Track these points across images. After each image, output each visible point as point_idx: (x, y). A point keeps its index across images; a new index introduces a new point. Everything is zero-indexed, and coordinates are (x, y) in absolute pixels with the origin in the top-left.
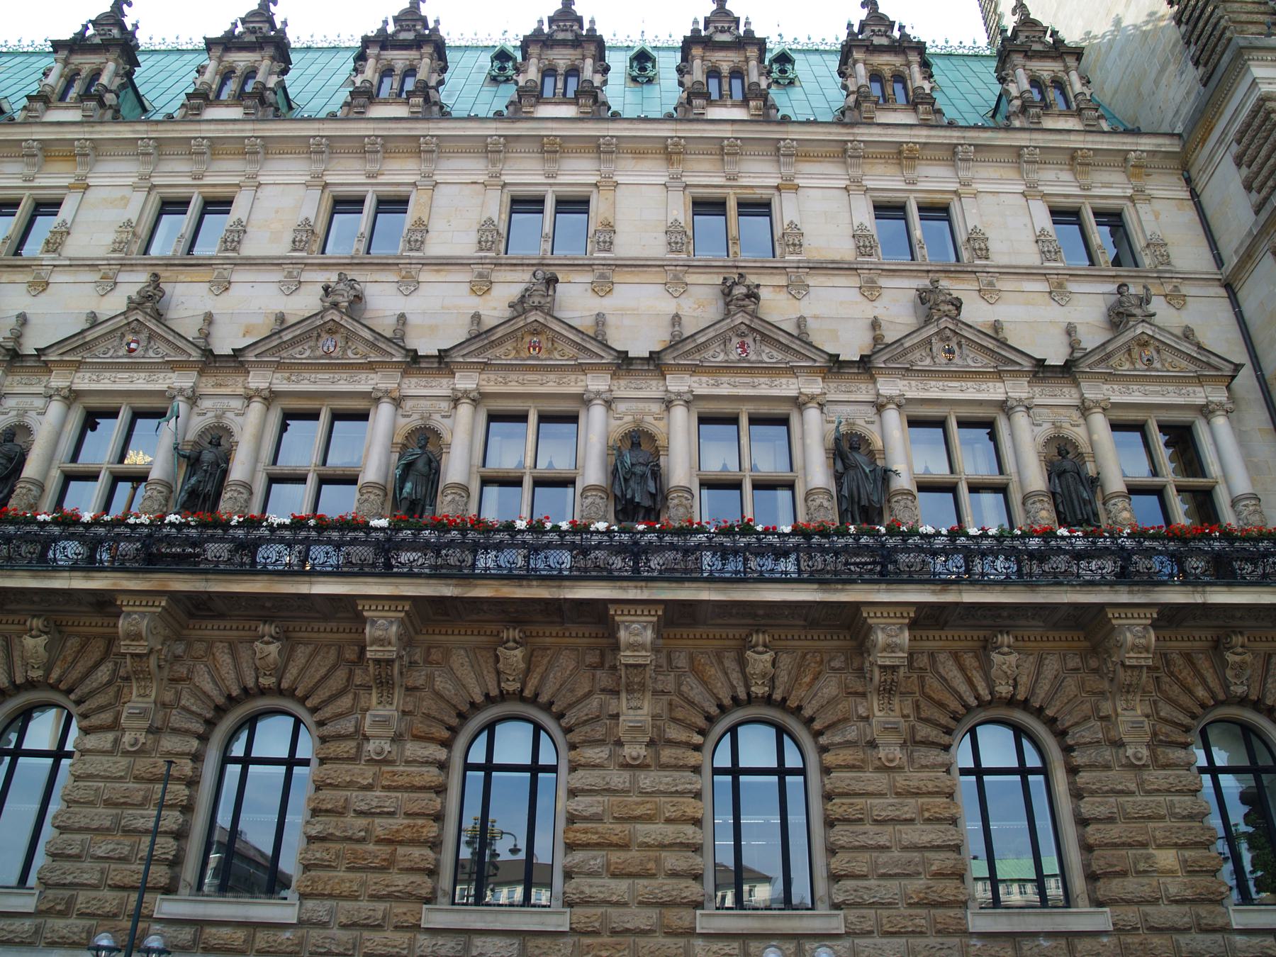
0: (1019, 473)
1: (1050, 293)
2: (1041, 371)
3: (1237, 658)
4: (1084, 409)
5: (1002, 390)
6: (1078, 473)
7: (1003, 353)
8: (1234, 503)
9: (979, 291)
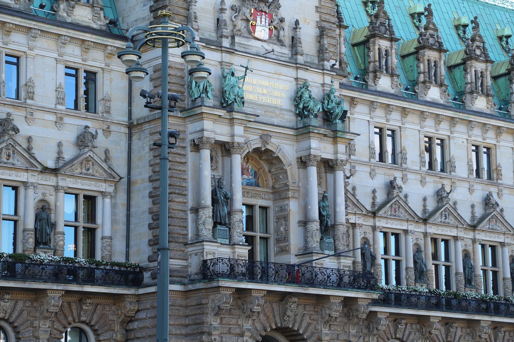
0: (24, 220)
1: (56, 122)
2: (45, 170)
3: (87, 308)
4: (57, 188)
5: (26, 177)
6: (48, 219)
7: (31, 160)
8: (103, 238)
9: (26, 117)
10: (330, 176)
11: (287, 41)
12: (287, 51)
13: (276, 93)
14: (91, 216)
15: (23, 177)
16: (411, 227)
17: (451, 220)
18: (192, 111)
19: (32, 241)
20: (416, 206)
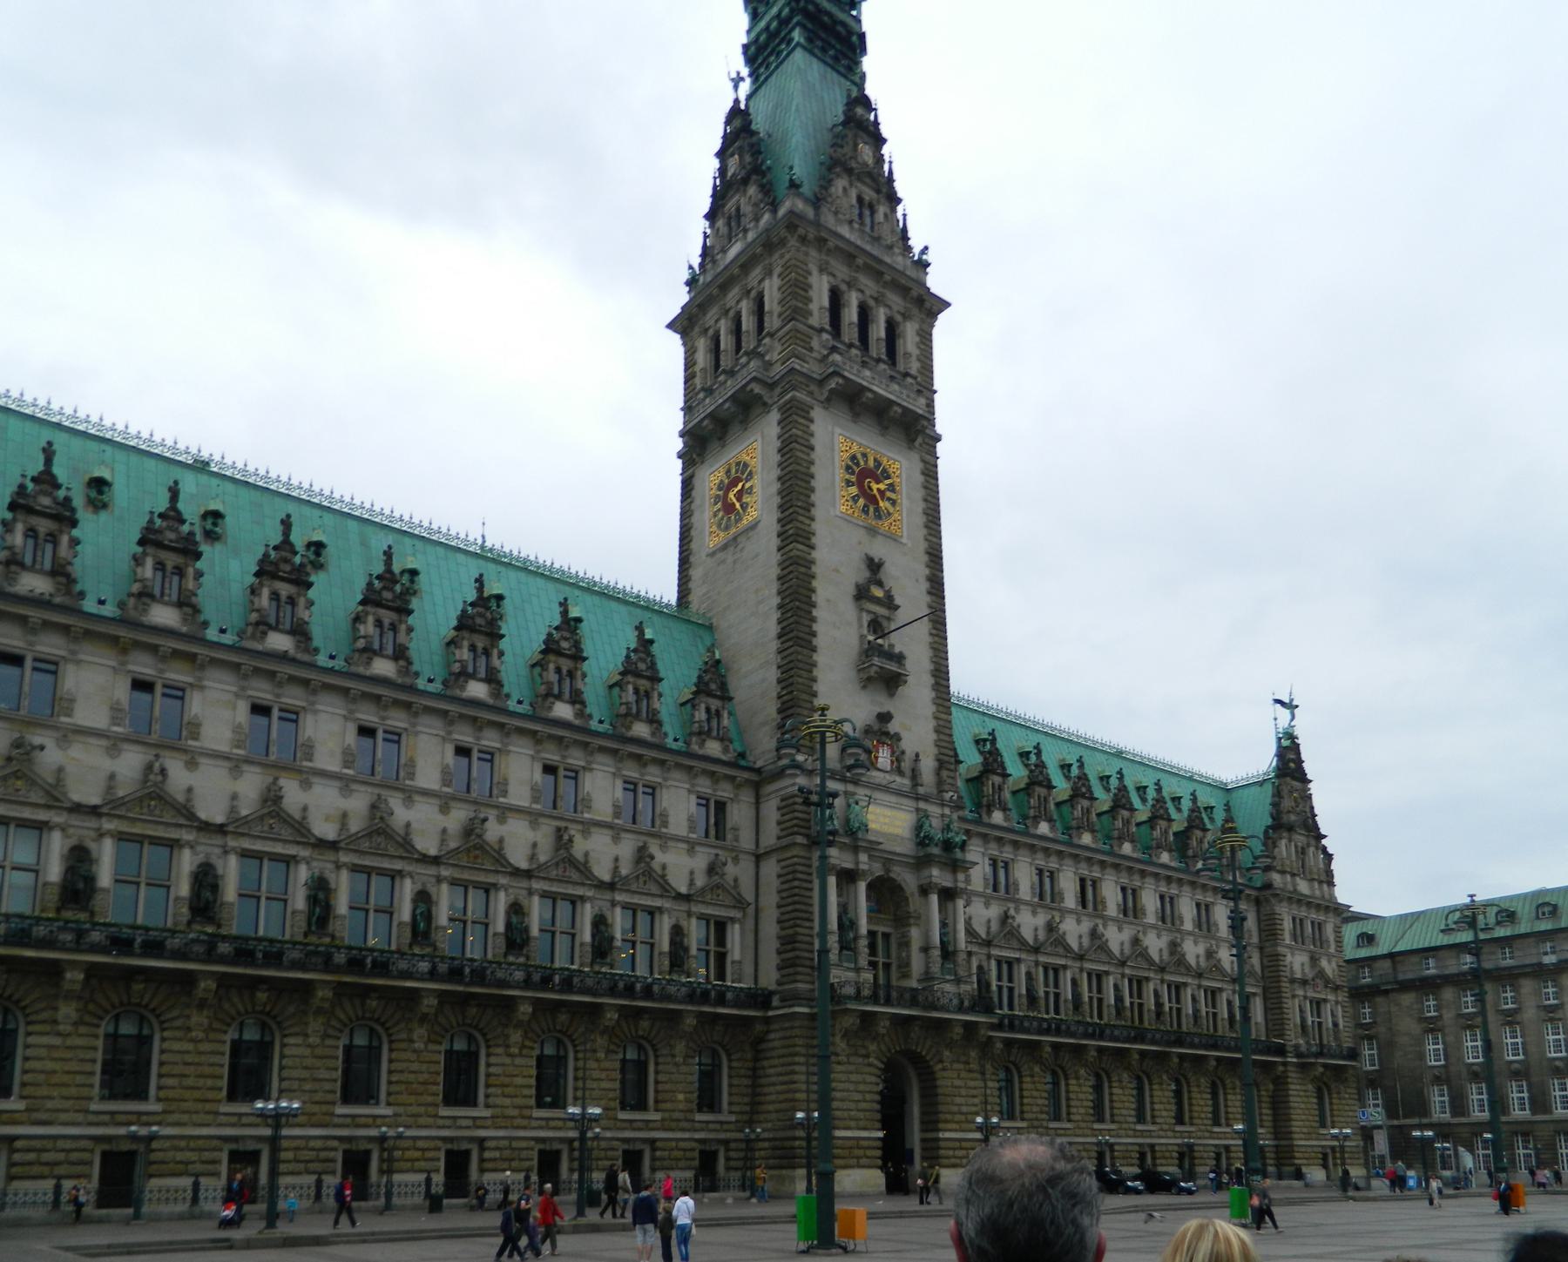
6: (681, 943)
10: (950, 905)
11: (908, 772)
12: (907, 782)
13: (898, 823)
14: (721, 940)
15: (658, 903)
16: (1024, 956)
17: (1061, 950)
18: (820, 841)
19: (667, 962)
20: (1028, 934)
